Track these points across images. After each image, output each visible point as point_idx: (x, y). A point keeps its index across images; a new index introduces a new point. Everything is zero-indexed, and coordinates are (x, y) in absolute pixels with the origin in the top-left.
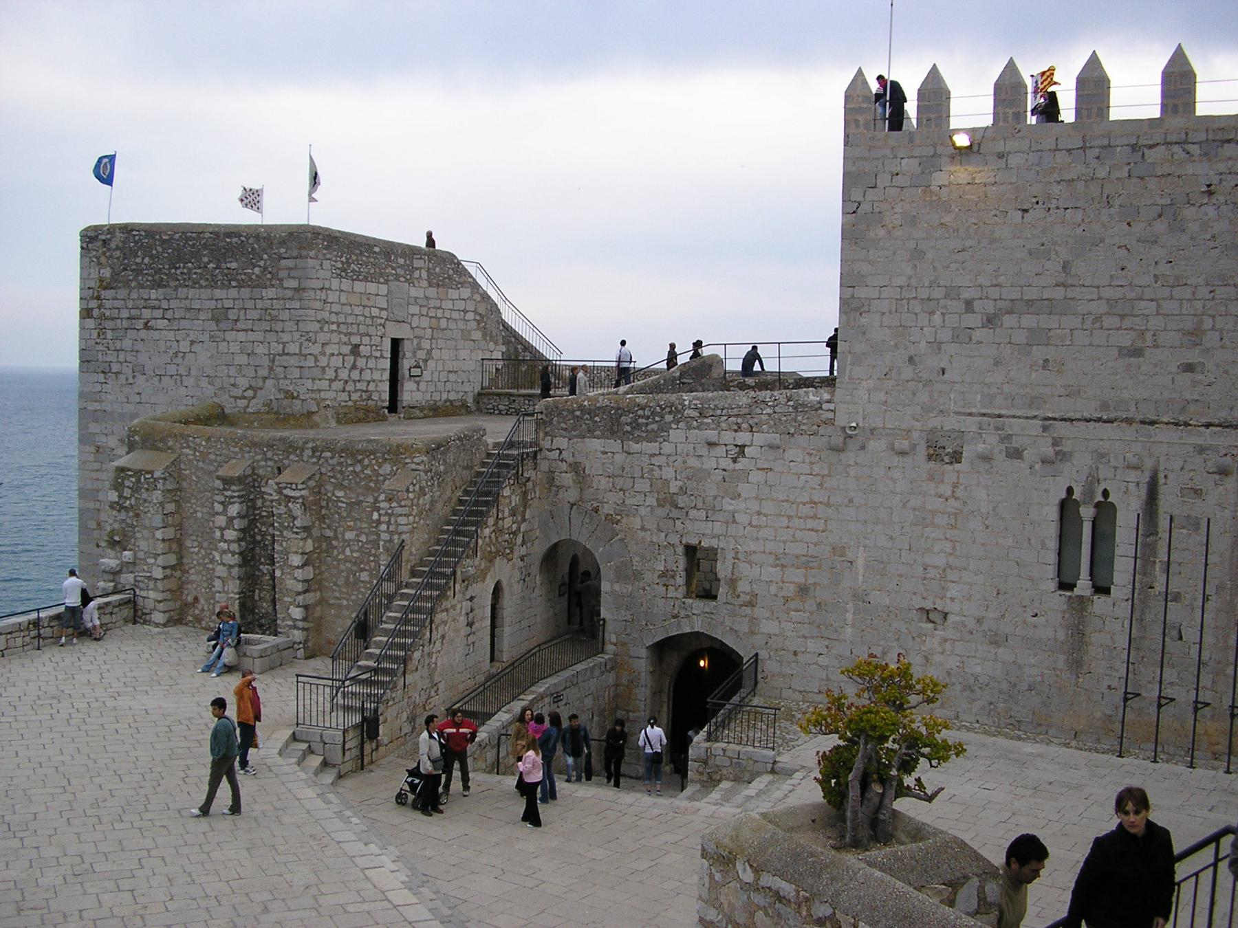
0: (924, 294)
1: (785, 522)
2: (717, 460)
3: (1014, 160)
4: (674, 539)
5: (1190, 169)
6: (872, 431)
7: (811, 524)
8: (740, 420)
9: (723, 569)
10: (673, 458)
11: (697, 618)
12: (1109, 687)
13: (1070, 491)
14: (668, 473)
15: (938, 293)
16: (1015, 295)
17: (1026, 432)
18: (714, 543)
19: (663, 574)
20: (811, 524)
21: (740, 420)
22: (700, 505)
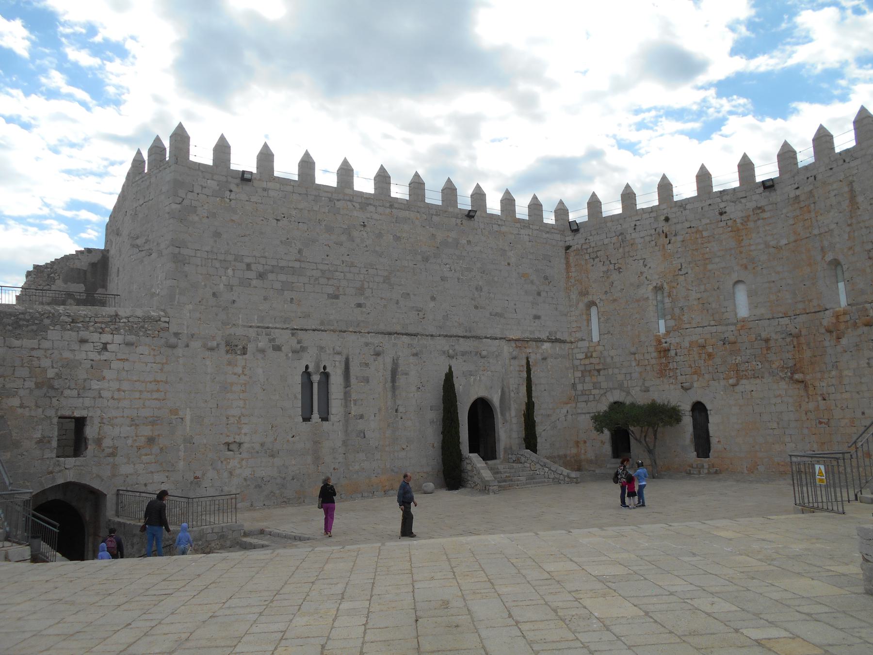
0: (222, 257)
1: (137, 395)
2: (87, 354)
3: (271, 193)
4: (51, 413)
5: (355, 214)
6: (193, 336)
7: (156, 395)
8: (103, 326)
9: (90, 431)
10: (50, 352)
11: (71, 470)
12: (334, 469)
13: (307, 367)
14: (46, 363)
15: (230, 258)
16: (274, 263)
17: (283, 337)
18: (83, 413)
19: (40, 441)
20: (156, 395)
21: (103, 326)
22: (73, 386)
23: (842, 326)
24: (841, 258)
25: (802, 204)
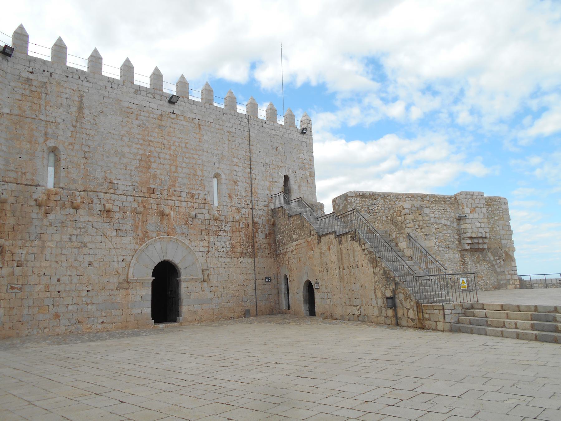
23: (52, 204)
24: (61, 147)
25: (33, 89)
